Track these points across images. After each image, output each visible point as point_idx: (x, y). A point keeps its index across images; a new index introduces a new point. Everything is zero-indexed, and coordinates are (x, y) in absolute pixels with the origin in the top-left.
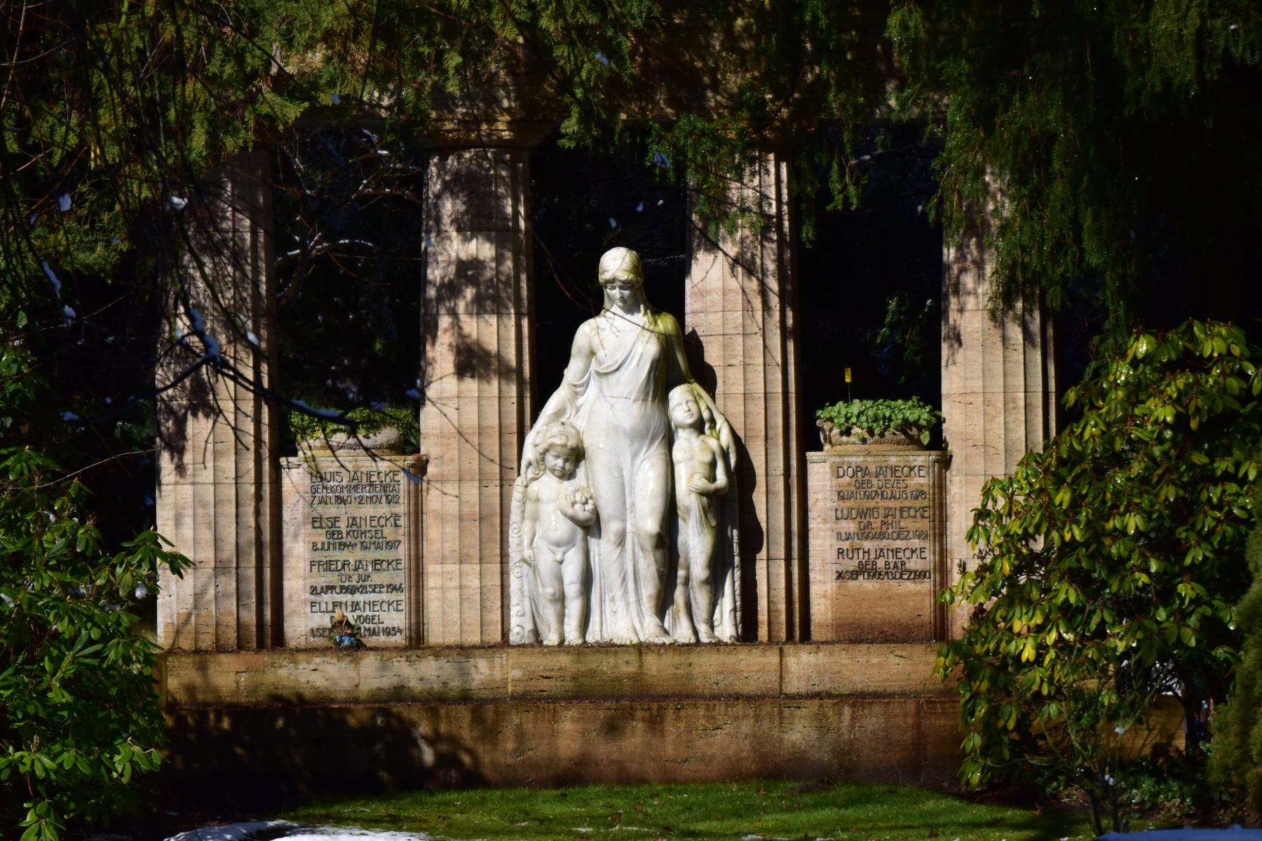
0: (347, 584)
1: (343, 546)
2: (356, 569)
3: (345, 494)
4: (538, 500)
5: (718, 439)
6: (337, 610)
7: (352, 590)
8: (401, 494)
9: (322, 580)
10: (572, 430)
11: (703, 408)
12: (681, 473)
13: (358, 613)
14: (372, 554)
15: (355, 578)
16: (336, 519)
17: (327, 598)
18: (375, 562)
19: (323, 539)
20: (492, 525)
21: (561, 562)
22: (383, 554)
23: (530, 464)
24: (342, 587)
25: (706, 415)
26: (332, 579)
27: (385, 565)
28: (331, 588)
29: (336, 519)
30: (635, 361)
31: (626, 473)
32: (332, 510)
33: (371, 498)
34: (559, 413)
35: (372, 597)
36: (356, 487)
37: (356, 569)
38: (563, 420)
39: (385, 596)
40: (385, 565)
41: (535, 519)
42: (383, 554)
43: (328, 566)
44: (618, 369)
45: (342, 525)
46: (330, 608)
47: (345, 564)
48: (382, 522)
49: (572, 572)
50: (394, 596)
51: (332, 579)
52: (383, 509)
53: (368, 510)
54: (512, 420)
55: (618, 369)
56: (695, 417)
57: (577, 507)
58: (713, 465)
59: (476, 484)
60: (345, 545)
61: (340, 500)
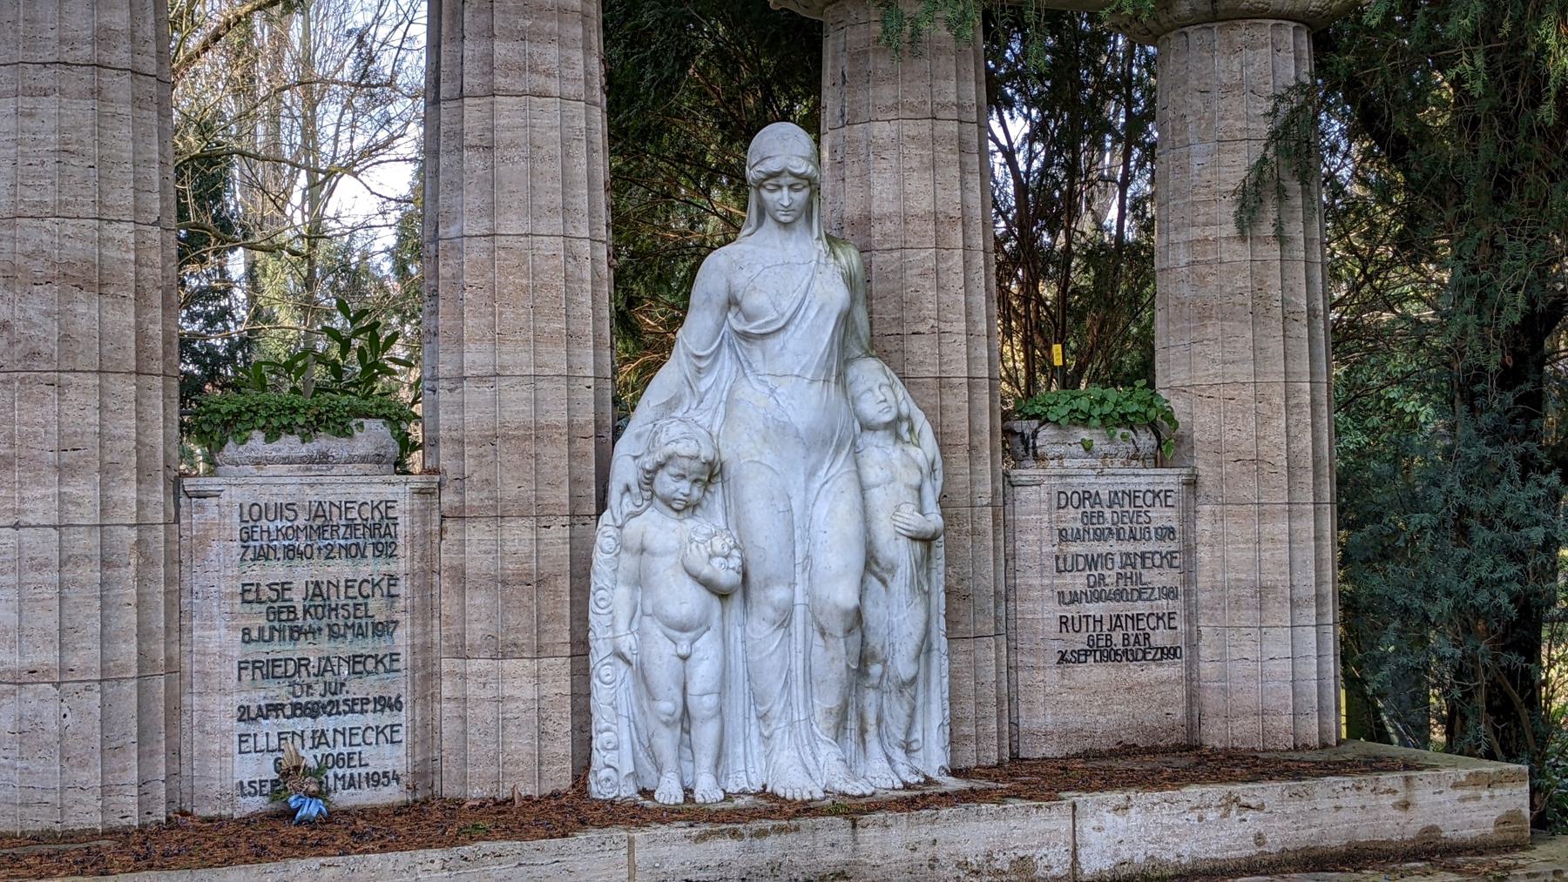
0: (304, 700)
1: (297, 633)
2: (320, 674)
3: (301, 543)
6: (288, 746)
7: (313, 711)
8: (400, 541)
9: (258, 697)
12: (878, 497)
13: (324, 749)
14: (347, 647)
15: (319, 688)
16: (285, 586)
17: (270, 726)
18: (354, 660)
19: (263, 622)
20: (556, 592)
22: (366, 646)
23: (628, 489)
24: (295, 706)
26: (278, 692)
27: (370, 664)
28: (275, 708)
29: (285, 586)
30: (812, 313)
32: (277, 571)
33: (347, 548)
34: (671, 405)
35: (349, 721)
36: (321, 531)
37: (320, 674)
38: (678, 414)
39: (370, 719)
40: (370, 664)
41: (639, 581)
42: (366, 646)
43: (268, 670)
44: (783, 328)
45: (297, 597)
46: (274, 743)
47: (302, 663)
48: (367, 589)
49: (704, 673)
50: (386, 718)
51: (278, 692)
52: (371, 567)
53: (341, 569)
54: (587, 416)
55: (783, 328)
57: (717, 561)
58: (919, 489)
60: (299, 630)
61: (292, 553)
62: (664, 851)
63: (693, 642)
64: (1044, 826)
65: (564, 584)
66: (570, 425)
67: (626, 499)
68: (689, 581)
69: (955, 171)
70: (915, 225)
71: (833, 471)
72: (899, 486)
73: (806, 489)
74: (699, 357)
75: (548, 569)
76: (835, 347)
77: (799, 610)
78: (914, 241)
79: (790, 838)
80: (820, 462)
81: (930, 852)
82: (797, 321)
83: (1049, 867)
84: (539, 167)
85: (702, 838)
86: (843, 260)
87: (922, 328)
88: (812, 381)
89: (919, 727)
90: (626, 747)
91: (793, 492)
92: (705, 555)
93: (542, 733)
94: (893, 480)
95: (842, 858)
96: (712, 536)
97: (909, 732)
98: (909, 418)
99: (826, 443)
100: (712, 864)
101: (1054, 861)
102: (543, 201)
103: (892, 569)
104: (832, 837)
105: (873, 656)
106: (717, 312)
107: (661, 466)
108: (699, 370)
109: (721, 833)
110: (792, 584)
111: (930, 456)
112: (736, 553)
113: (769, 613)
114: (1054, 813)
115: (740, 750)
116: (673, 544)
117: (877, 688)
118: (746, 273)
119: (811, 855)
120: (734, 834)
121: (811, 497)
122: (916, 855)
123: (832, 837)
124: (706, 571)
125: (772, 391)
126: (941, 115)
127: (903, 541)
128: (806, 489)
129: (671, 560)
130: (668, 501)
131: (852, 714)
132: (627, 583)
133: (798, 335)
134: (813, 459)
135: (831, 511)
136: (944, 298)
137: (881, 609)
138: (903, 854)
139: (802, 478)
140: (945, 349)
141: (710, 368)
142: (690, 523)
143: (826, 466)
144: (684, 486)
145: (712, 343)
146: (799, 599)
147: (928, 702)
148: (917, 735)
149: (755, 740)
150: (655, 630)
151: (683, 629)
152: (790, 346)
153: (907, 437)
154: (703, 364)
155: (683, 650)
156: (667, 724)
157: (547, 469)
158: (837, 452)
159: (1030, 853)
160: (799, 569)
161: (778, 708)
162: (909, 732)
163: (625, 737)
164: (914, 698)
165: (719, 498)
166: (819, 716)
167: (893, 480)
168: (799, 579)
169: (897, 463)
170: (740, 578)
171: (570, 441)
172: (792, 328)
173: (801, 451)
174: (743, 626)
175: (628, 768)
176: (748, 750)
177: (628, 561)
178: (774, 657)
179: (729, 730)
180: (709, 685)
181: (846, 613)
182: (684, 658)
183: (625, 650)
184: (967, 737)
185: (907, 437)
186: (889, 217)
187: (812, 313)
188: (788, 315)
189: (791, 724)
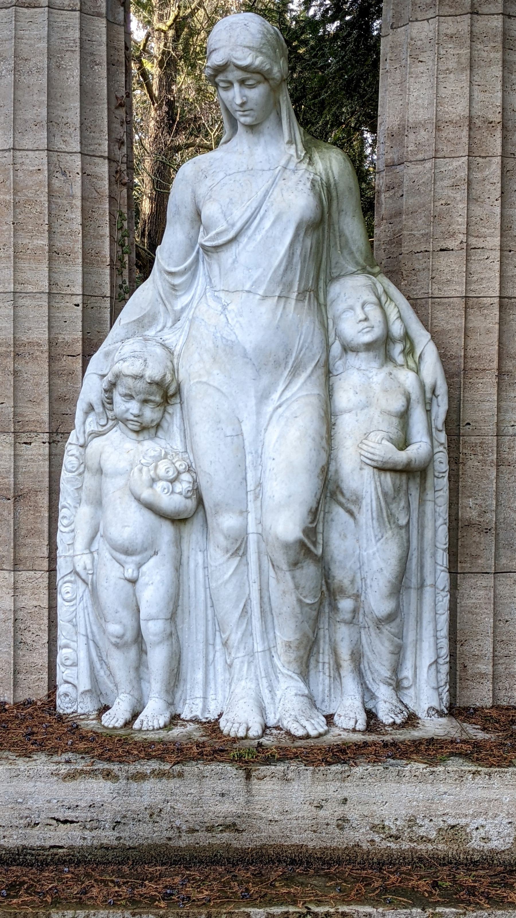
4: (100, 471)
5: (418, 372)
10: (159, 350)
11: (393, 315)
20: (36, 508)
21: (133, 582)
23: (91, 408)
25: (397, 329)
30: (267, 224)
31: (247, 428)
38: (151, 333)
44: (234, 239)
55: (234, 239)
56: (377, 332)
57: (160, 486)
59: (10, 438)
62: (28, 786)
63: (139, 566)
64: (481, 794)
65: (44, 500)
66: (52, 343)
67: (91, 418)
68: (134, 504)
69: (497, 71)
70: (448, 132)
71: (288, 394)
72: (374, 412)
73: (258, 413)
74: (171, 273)
75: (26, 484)
76: (297, 259)
77: (252, 539)
78: (446, 149)
79: (173, 784)
80: (273, 385)
81: (340, 811)
82: (250, 232)
83: (486, 839)
84: (25, 80)
85: (71, 776)
86: (320, 166)
87: (451, 244)
88: (265, 297)
89: (409, 664)
90: (83, 664)
91: (243, 415)
92: (145, 477)
93: (17, 644)
94: (367, 405)
95: (233, 809)
96: (158, 459)
97: (396, 669)
98: (407, 337)
99: (278, 364)
100: (82, 804)
101: (493, 833)
102: (29, 115)
103: (357, 500)
104: (221, 786)
105: (342, 591)
106: (187, 226)
107: (113, 385)
108: (174, 287)
109: (92, 773)
110: (244, 513)
111: (428, 381)
112: (186, 477)
113: (221, 540)
114: (496, 780)
115: (200, 676)
116: (123, 465)
117: (351, 622)
118: (208, 182)
119: (197, 803)
120: (108, 775)
121: (264, 421)
122: (322, 813)
123: (221, 786)
124: (146, 494)
125: (224, 308)
126: (485, 9)
127: (368, 472)
128: (258, 413)
129: (120, 481)
130: (125, 421)
131: (324, 647)
132: (89, 502)
133: (251, 246)
134: (265, 380)
135: (282, 436)
136: (477, 211)
137: (349, 543)
138: (308, 811)
139: (252, 402)
140: (474, 267)
141: (189, 285)
142: (148, 445)
143: (280, 389)
144: (134, 407)
145: (185, 259)
146: (251, 528)
147: (418, 641)
148: (407, 672)
149: (220, 666)
150: (106, 554)
151: (127, 552)
152: (242, 259)
153: (400, 359)
154: (177, 281)
155: (130, 573)
156: (116, 645)
157: (29, 386)
158: (295, 372)
159: (463, 821)
160: (250, 497)
161: (235, 638)
162: (396, 669)
163: (82, 654)
164: (400, 635)
165: (177, 420)
166: (280, 648)
167: (367, 405)
168: (251, 507)
169: (377, 388)
170: (191, 504)
171: (51, 358)
172: (244, 240)
173: (250, 372)
174: (205, 551)
175: (84, 684)
176: (211, 676)
177: (89, 480)
178: (230, 587)
179: (187, 656)
180: (154, 611)
181: (287, 546)
182: (133, 582)
183: (79, 569)
184: (483, 675)
185: (400, 359)
186: (423, 125)
187: (267, 224)
188: (238, 226)
189: (252, 654)
